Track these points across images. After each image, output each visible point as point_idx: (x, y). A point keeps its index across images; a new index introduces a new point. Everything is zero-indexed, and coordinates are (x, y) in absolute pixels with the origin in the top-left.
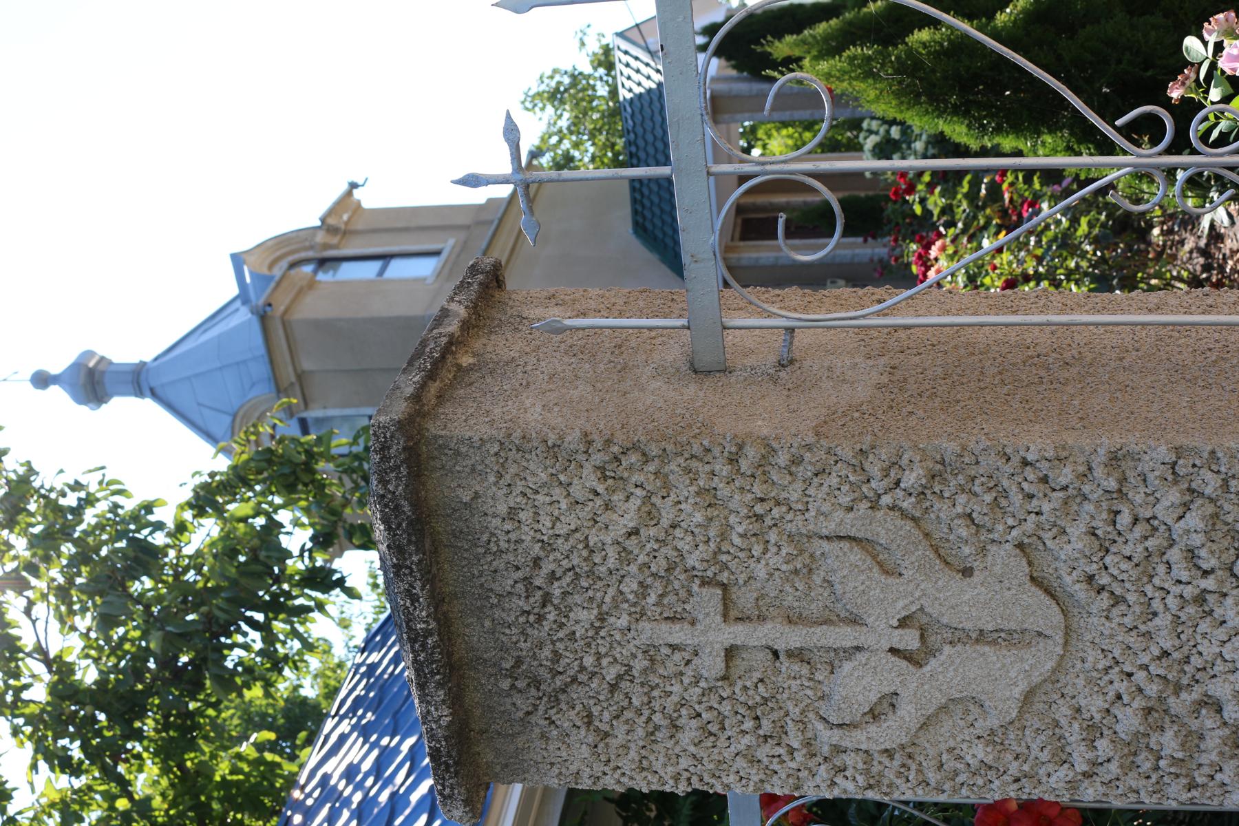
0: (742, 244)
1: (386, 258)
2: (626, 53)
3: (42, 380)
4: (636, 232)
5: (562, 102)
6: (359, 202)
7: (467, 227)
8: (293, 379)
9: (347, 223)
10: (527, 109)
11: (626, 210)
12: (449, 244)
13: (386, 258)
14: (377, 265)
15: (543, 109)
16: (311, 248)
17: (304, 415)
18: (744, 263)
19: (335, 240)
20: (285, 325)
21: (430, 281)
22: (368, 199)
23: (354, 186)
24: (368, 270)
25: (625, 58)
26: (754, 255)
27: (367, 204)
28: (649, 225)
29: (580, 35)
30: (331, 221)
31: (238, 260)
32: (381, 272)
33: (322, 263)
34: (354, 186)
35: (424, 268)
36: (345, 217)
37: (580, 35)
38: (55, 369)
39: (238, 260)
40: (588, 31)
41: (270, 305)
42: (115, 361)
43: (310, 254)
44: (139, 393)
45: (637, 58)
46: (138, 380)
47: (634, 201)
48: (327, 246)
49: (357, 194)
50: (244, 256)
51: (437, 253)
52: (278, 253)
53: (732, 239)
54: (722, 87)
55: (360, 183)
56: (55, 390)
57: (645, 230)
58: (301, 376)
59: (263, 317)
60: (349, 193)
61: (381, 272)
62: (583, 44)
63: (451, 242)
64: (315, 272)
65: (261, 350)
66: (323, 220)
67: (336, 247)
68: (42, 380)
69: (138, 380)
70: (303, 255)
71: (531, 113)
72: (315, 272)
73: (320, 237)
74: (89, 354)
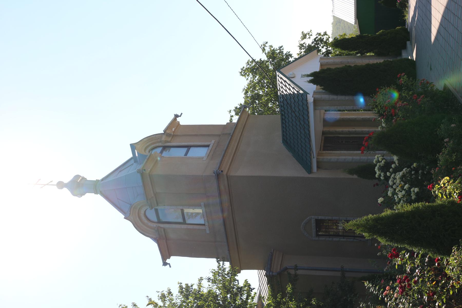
0: (324, 152)
1: (189, 147)
2: (281, 78)
3: (61, 185)
4: (283, 143)
5: (256, 73)
6: (179, 122)
7: (220, 135)
8: (153, 196)
10: (242, 75)
11: (280, 133)
12: (212, 142)
13: (189, 147)
14: (185, 150)
15: (248, 75)
16: (161, 142)
17: (157, 208)
19: (169, 139)
21: (204, 159)
22: (182, 121)
23: (176, 116)
24: (181, 152)
25: (280, 80)
26: (329, 158)
27: (181, 123)
30: (168, 132)
31: (133, 146)
32: (186, 154)
33: (165, 148)
34: (176, 116)
35: (201, 153)
36: (173, 130)
37: (263, 46)
39: (133, 146)
40: (267, 45)
41: (145, 170)
42: (88, 179)
43: (160, 144)
44: (96, 193)
45: (285, 81)
46: (97, 187)
49: (178, 119)
50: (135, 145)
51: (208, 146)
52: (148, 144)
53: (320, 150)
54: (318, 96)
55: (179, 115)
56: (65, 190)
57: (287, 143)
59: (142, 173)
61: (186, 154)
63: (213, 142)
64: (161, 152)
65: (141, 184)
66: (165, 131)
67: (168, 142)
68: (61, 185)
69: (97, 187)
70: (157, 145)
71: (244, 77)
72: (161, 152)
73: (164, 138)
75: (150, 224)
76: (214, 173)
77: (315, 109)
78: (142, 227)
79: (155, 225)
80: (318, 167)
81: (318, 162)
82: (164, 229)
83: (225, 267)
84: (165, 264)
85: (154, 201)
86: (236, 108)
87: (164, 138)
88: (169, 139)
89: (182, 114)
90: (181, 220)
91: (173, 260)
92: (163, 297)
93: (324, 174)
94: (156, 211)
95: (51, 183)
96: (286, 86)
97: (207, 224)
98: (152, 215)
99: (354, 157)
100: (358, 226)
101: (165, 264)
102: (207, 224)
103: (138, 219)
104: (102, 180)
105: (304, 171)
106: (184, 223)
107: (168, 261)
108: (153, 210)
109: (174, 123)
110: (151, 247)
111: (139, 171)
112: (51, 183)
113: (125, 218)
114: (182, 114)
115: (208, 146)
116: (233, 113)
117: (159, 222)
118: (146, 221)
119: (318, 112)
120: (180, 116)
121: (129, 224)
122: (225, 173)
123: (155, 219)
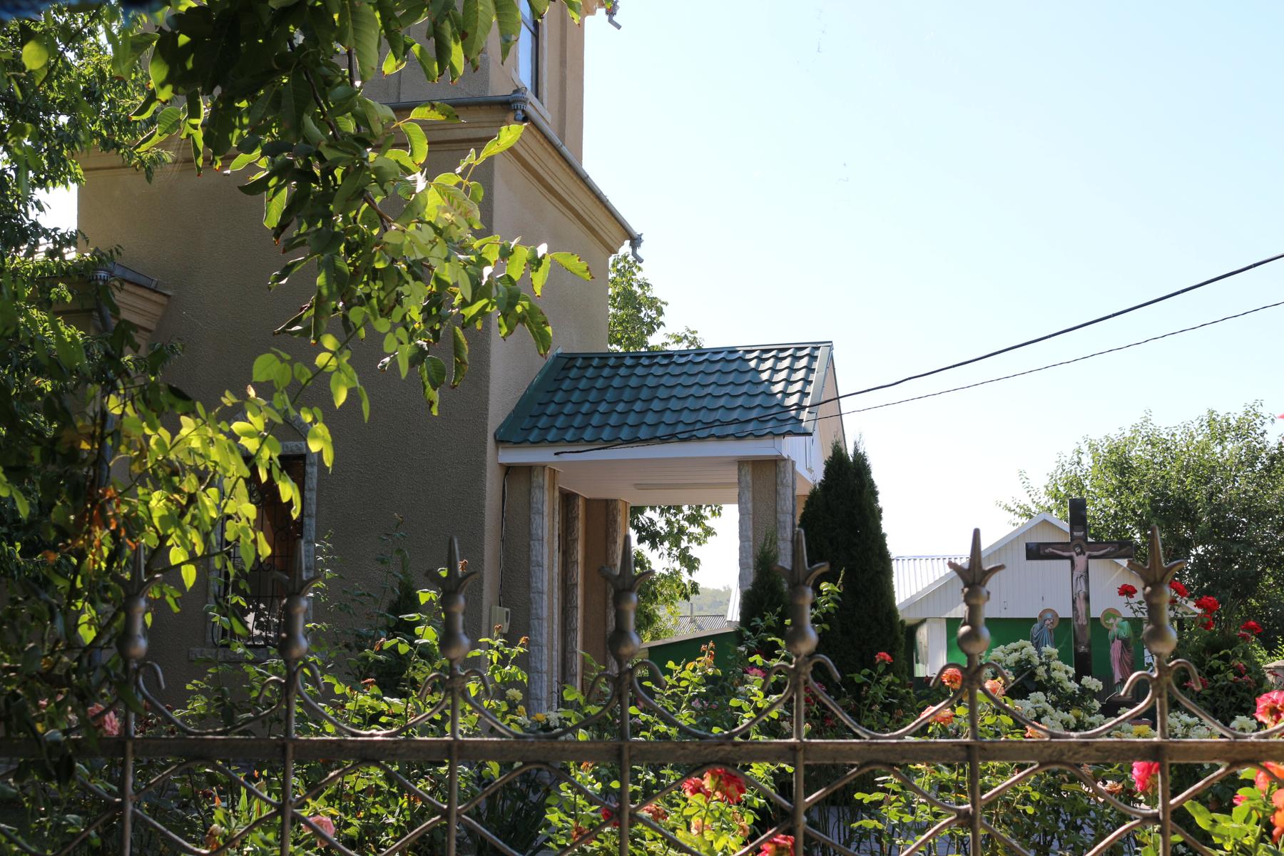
6: (593, 12)
18: (537, 494)
28: (573, 373)
29: (691, 337)
37: (691, 337)
47: (588, 358)
57: (566, 368)
62: (679, 340)
63: (548, 117)
76: (515, 92)
77: (742, 463)
80: (509, 471)
81: (528, 469)
89: (619, 27)
93: (492, 483)
96: (792, 370)
99: (545, 597)
105: (501, 420)
114: (619, 27)
119: (732, 475)
120: (611, 21)
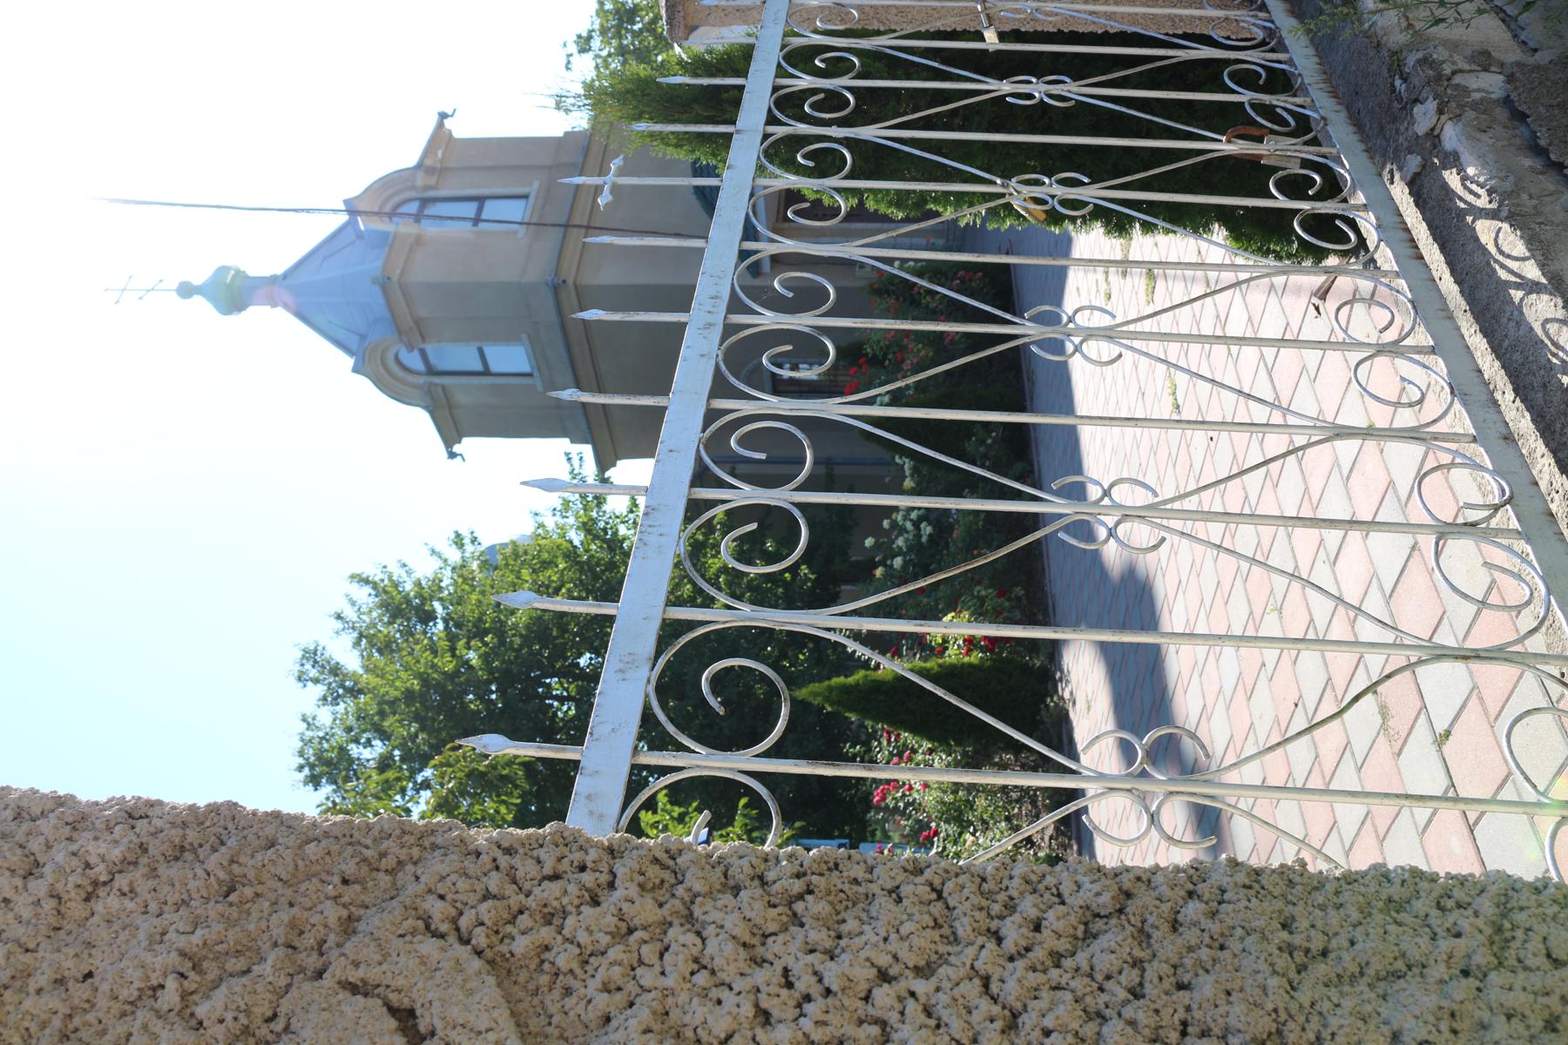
1: (481, 200)
3: (186, 291)
7: (550, 168)
8: (411, 324)
9: (441, 161)
12: (534, 187)
16: (413, 187)
19: (433, 181)
20: (403, 287)
22: (460, 129)
27: (457, 134)
30: (428, 162)
33: (425, 202)
38: (199, 279)
43: (413, 194)
44: (274, 305)
48: (427, 188)
49: (448, 123)
51: (526, 197)
58: (418, 323)
59: (384, 284)
60: (440, 125)
63: (536, 184)
68: (186, 291)
70: (407, 195)
73: (420, 180)
74: (223, 270)
75: (410, 378)
78: (393, 382)
79: (421, 380)
82: (443, 387)
83: (584, 473)
84: (452, 455)
85: (415, 331)
86: (579, 37)
87: (420, 180)
88: (433, 181)
90: (479, 367)
91: (468, 445)
92: (458, 541)
94: (423, 354)
95: (161, 286)
97: (536, 374)
98: (414, 361)
100: (816, 694)
101: (452, 455)
102: (536, 374)
103: (382, 370)
104: (285, 276)
106: (486, 372)
107: (456, 448)
108: (416, 353)
109: (440, 136)
110: (418, 422)
111: (375, 281)
112: (161, 286)
113: (355, 370)
115: (526, 197)
116: (573, 49)
117: (431, 371)
118: (401, 373)
121: (364, 384)
122: (570, 282)
123: (420, 367)
